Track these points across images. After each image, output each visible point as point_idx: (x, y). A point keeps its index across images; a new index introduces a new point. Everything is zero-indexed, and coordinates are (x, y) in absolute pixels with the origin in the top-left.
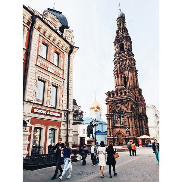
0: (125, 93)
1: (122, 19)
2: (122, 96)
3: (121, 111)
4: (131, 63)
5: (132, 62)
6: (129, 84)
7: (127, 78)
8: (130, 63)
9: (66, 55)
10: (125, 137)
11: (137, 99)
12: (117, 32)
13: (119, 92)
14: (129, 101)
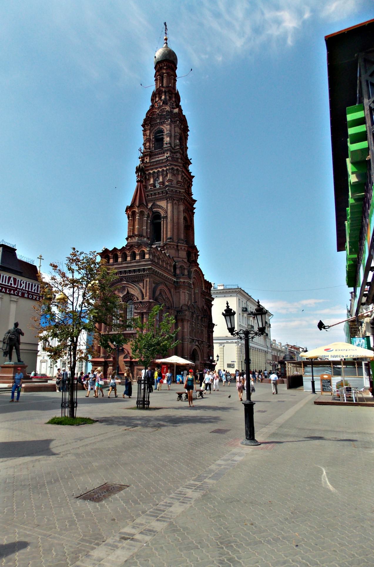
0: (143, 255)
2: (133, 262)
3: (128, 297)
5: (180, 179)
6: (167, 234)
7: (164, 218)
8: (175, 182)
10: (129, 360)
11: (178, 271)
12: (152, 100)
14: (147, 276)
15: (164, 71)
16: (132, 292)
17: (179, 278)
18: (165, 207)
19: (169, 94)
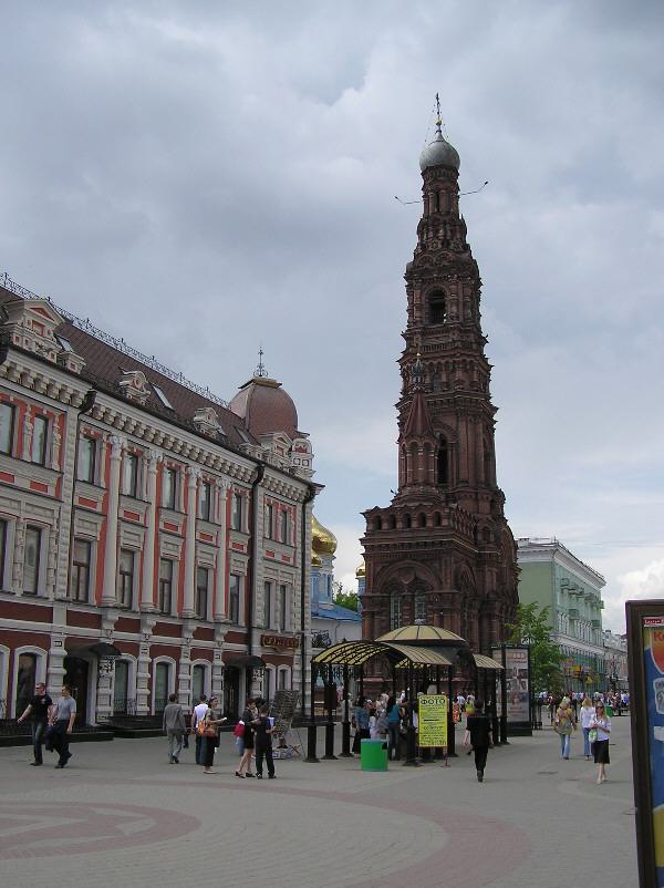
1: (441, 174)
3: (418, 585)
4: (472, 383)
8: (467, 383)
9: (299, 507)
11: (480, 537)
13: (415, 516)
15: (441, 186)
16: (423, 577)
17: (483, 549)
18: (454, 426)
19: (451, 225)
